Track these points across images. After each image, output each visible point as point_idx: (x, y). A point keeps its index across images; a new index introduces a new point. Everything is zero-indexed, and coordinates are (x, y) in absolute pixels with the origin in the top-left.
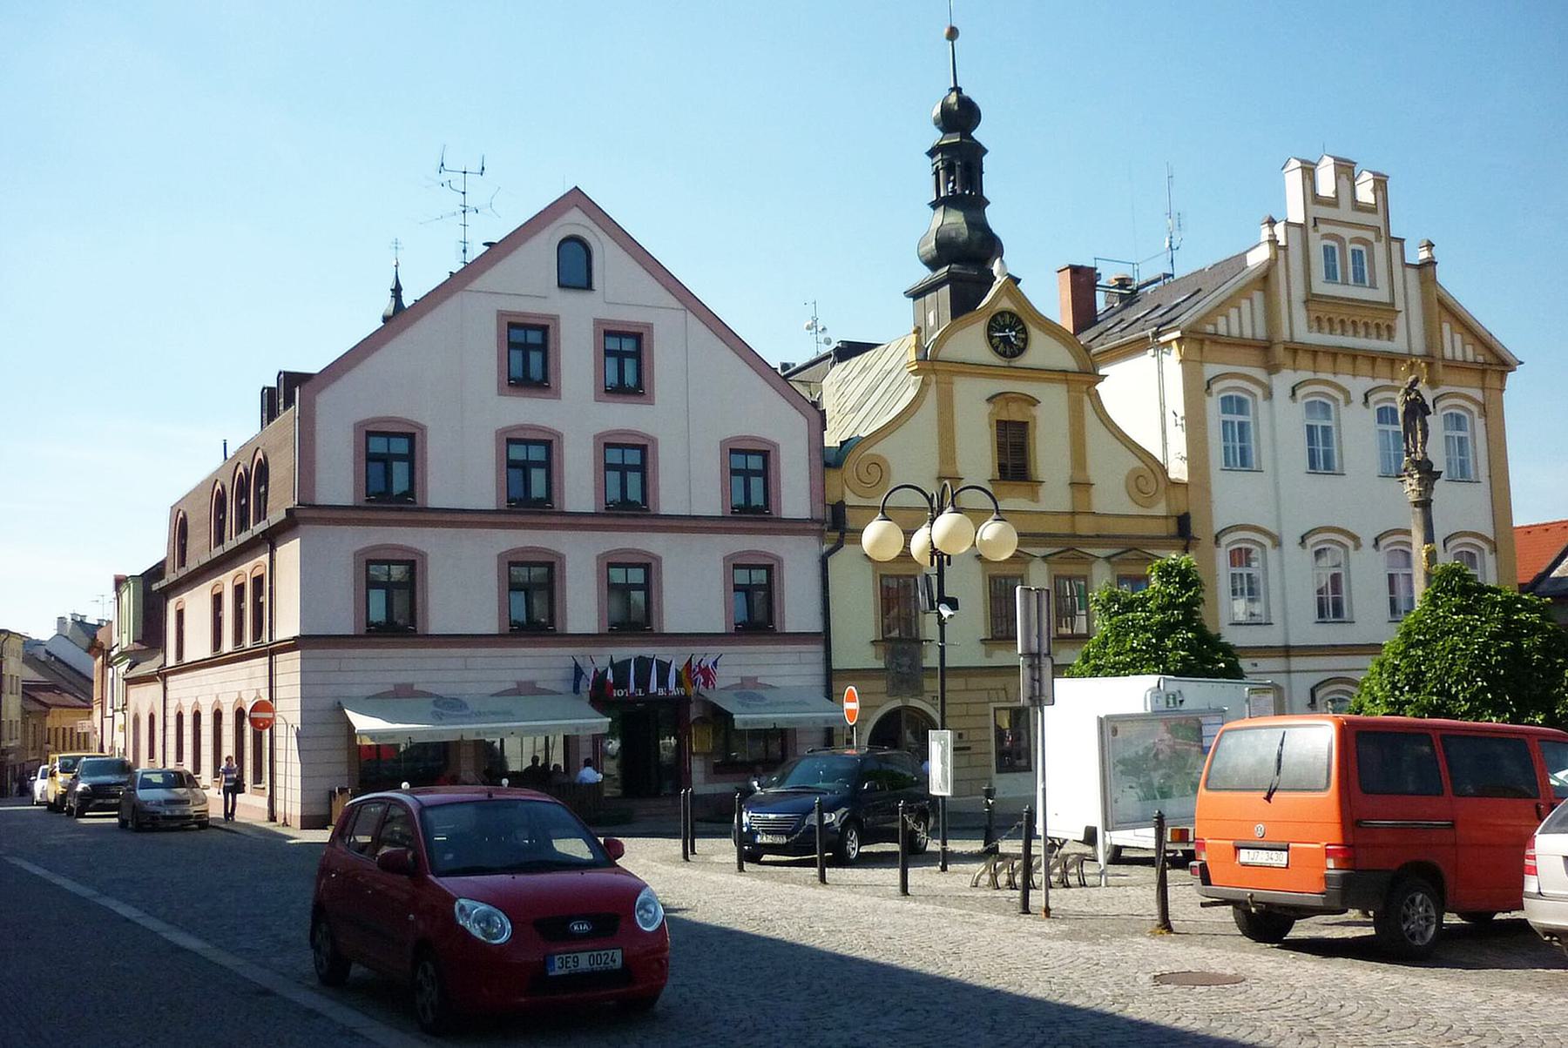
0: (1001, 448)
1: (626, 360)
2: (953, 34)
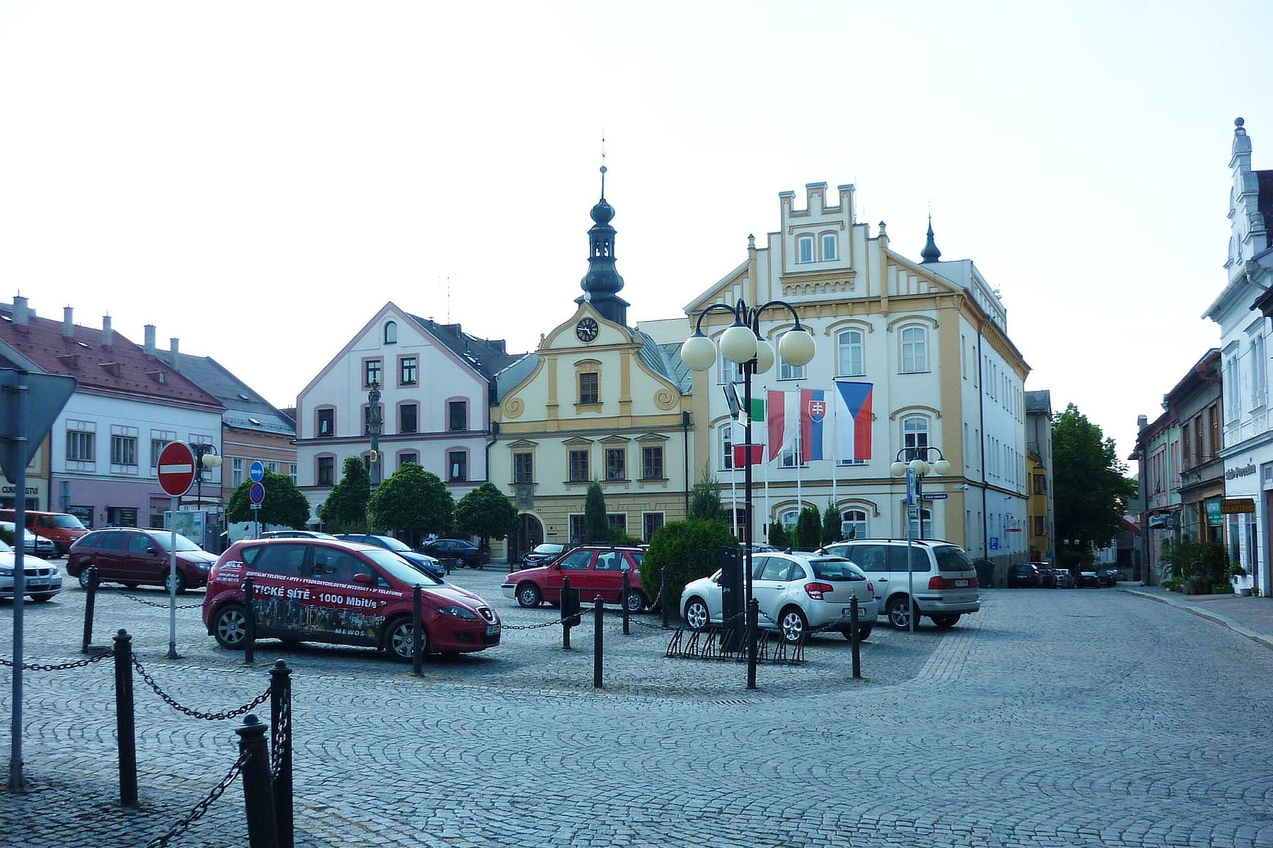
0: (583, 387)
1: (407, 369)
2: (603, 169)
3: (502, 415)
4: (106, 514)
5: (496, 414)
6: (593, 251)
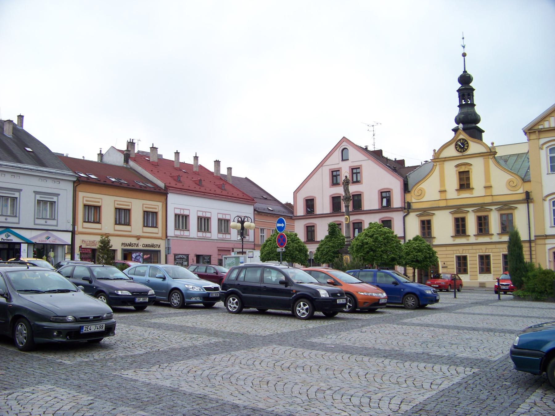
0: (460, 179)
2: (464, 55)
3: (412, 198)
4: (195, 259)
5: (409, 197)
6: (460, 101)
